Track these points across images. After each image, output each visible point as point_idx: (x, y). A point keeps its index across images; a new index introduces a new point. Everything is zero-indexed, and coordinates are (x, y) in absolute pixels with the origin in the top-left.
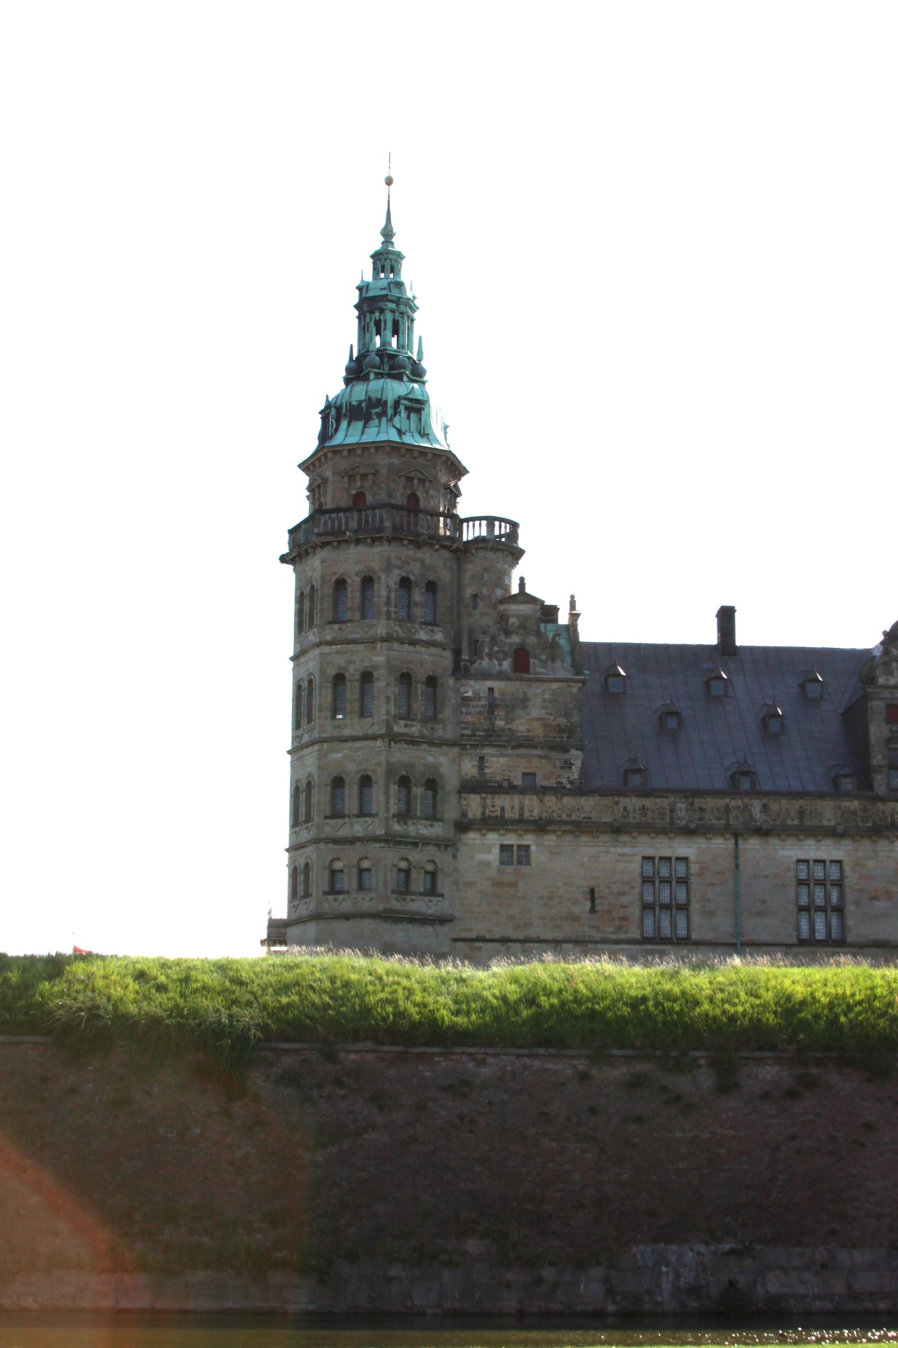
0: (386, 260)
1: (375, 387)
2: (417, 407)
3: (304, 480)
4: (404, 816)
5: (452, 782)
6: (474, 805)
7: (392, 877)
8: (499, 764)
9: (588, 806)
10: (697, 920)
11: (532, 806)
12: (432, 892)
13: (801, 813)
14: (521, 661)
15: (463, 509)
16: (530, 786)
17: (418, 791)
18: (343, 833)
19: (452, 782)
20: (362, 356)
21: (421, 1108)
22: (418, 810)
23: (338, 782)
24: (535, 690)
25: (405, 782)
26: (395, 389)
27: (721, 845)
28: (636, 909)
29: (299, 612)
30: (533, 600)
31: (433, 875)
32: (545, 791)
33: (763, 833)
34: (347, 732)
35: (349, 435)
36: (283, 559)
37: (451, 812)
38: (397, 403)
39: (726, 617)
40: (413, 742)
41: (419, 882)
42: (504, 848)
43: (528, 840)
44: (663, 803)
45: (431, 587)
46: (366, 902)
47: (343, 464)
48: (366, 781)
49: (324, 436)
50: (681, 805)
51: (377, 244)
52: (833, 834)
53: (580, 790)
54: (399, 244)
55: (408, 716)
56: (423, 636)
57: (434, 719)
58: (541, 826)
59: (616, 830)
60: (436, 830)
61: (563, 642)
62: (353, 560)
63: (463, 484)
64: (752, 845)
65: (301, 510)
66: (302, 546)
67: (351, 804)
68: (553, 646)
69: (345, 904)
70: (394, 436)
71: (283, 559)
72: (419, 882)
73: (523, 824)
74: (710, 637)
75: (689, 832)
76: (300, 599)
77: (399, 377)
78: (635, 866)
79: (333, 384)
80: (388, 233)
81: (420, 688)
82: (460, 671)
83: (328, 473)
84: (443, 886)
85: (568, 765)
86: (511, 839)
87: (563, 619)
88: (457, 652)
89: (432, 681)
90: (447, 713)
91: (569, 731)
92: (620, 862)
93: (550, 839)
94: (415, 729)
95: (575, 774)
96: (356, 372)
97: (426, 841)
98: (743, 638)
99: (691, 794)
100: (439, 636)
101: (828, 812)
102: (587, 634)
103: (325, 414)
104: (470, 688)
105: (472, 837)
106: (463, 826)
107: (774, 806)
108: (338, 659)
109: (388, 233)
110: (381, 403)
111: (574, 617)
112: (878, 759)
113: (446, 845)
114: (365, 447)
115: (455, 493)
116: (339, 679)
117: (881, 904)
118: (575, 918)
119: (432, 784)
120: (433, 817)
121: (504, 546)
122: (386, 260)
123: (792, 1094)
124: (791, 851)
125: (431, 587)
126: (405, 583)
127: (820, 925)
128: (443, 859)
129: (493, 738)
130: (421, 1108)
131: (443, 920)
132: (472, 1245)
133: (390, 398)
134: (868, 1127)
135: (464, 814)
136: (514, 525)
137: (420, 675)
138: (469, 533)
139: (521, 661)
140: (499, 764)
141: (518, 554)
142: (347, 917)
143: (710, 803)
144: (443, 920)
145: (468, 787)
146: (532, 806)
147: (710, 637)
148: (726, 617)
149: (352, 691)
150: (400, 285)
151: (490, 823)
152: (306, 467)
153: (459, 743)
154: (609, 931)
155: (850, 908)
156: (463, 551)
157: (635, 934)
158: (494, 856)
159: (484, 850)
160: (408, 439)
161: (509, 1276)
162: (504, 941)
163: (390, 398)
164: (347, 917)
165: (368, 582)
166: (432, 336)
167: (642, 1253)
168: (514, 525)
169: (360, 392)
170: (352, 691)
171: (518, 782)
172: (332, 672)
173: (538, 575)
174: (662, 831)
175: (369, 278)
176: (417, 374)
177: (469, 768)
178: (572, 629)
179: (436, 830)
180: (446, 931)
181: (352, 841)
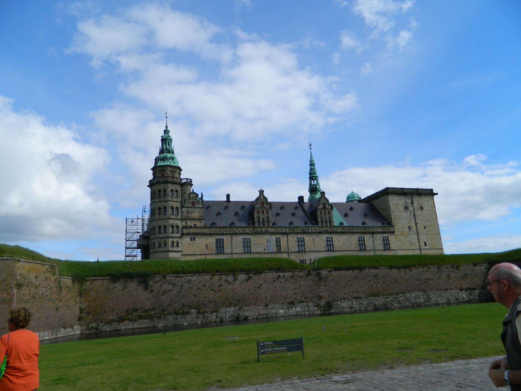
0: (166, 132)
1: (165, 154)
2: (173, 158)
3: (152, 172)
4: (173, 232)
5: (180, 227)
6: (185, 231)
7: (170, 244)
8: (189, 223)
9: (206, 231)
10: (225, 249)
12: (178, 246)
13: (243, 230)
15: (182, 177)
17: (175, 228)
18: (161, 236)
19: (180, 227)
20: (162, 149)
21: (182, 286)
22: (175, 232)
23: (160, 227)
24: (196, 209)
25: (172, 227)
26: (169, 155)
28: (215, 248)
29: (151, 196)
30: (195, 193)
31: (178, 244)
32: (198, 228)
33: (236, 234)
34: (162, 218)
35: (160, 164)
36: (148, 186)
38: (169, 158)
39: (228, 196)
40: (174, 219)
41: (175, 245)
42: (191, 238)
43: (195, 236)
44: (219, 229)
45: (177, 191)
46: (166, 249)
47: (160, 169)
48: (165, 227)
49: (156, 163)
50: (222, 229)
51: (165, 129)
52: (249, 234)
53: (205, 227)
54: (169, 129)
55: (173, 214)
56: (175, 200)
57: (178, 215)
59: (210, 234)
60: (179, 235)
61: (200, 201)
63: (181, 172)
66: (152, 184)
67: (163, 231)
68: (199, 202)
69: (161, 250)
70: (169, 164)
71: (148, 186)
72: (175, 245)
74: (226, 200)
75: (223, 234)
76: (151, 193)
77: (170, 153)
78: (214, 240)
79: (157, 154)
80: (166, 127)
81: (175, 210)
83: (157, 171)
84: (180, 245)
85: (202, 223)
86: (192, 236)
87: (200, 196)
88: (181, 203)
89: (177, 208)
90: (180, 214)
91: (202, 217)
92: (212, 240)
93: (199, 236)
94: (174, 217)
95: (203, 224)
96: (162, 152)
97: (176, 237)
98: (231, 200)
99: (223, 228)
100: (178, 200)
101: (247, 230)
102: (205, 199)
103: (156, 160)
104: (184, 210)
105: (184, 236)
106: (183, 234)
107: (238, 229)
108: (159, 205)
109: (166, 127)
110: (166, 158)
111: (202, 196)
112: (256, 220)
113: (180, 238)
114: (164, 166)
115: (180, 174)
116: (160, 208)
117: (257, 246)
118: (204, 250)
119: (177, 227)
120: (178, 233)
121: (189, 183)
122: (166, 132)
123: (248, 280)
124: (241, 238)
125: (177, 191)
126: (172, 190)
127: (246, 250)
128: (180, 240)
129: (188, 219)
130: (182, 286)
131: (180, 252)
132: (193, 311)
133: (168, 157)
134: (261, 285)
135: (183, 232)
136: (191, 180)
137: (175, 207)
138: (183, 181)
140: (189, 223)
141: (192, 185)
142: (162, 252)
143: (227, 229)
144: (180, 252)
145: (183, 227)
146: (195, 231)
148: (228, 196)
149: (162, 210)
150: (169, 136)
151: (188, 234)
152: (152, 169)
153: (182, 220)
154: (210, 252)
155: (252, 246)
156: (182, 185)
157: (214, 252)
158: (189, 239)
159: (187, 240)
160: (172, 164)
161: (199, 316)
162: (191, 255)
163: (168, 157)
164: (162, 252)
165: (165, 190)
166: (175, 145)
167: (223, 310)
168: (191, 180)
169: (162, 155)
170: (162, 210)
171: (193, 226)
172: (158, 207)
173: (196, 188)
174: (219, 234)
175: (163, 135)
176: (173, 153)
177: (184, 224)
178: (202, 198)
179: (179, 235)
180: (180, 253)
181: (163, 238)
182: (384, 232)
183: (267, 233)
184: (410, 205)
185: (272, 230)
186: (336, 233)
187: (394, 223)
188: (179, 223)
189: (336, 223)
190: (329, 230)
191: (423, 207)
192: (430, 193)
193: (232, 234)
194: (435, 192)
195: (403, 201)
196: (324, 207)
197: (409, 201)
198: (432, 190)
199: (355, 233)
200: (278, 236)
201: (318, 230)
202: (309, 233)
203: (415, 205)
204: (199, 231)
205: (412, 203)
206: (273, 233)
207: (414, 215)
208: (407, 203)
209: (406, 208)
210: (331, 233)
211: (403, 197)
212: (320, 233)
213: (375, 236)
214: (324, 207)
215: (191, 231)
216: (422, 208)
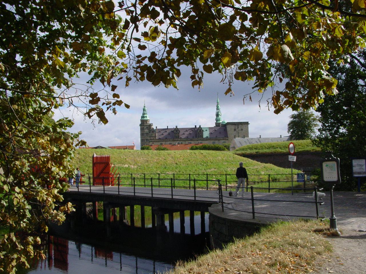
6: (150, 141)
8: (152, 138)
11: (153, 140)
14: (153, 132)
16: (154, 139)
27: (164, 142)
37: (149, 141)
39: (168, 126)
58: (154, 142)
62: (143, 127)
64: (166, 142)
65: (140, 123)
73: (153, 141)
82: (149, 133)
89: (148, 133)
98: (168, 128)
104: (150, 134)
106: (150, 142)
139: (153, 132)
145: (150, 139)
146: (153, 140)
147: (167, 128)
148: (168, 126)
151: (151, 141)
153: (149, 137)
182: (223, 140)
183: (178, 140)
184: (237, 128)
185: (180, 140)
186: (204, 140)
187: (228, 136)
188: (148, 138)
189: (204, 136)
190: (201, 139)
191: (243, 129)
192: (247, 123)
193: (166, 141)
194: (249, 123)
195: (234, 127)
196: (200, 131)
197: (237, 127)
198: (248, 122)
199: (212, 140)
200: (182, 142)
201: (197, 139)
202: (193, 140)
203: (239, 129)
204: (155, 140)
205: (238, 127)
206: (180, 141)
207: (238, 133)
208: (235, 128)
209: (235, 130)
210: (202, 140)
211: (234, 126)
212: (197, 140)
213: (220, 141)
214: (200, 131)
215: (152, 140)
216: (242, 130)
